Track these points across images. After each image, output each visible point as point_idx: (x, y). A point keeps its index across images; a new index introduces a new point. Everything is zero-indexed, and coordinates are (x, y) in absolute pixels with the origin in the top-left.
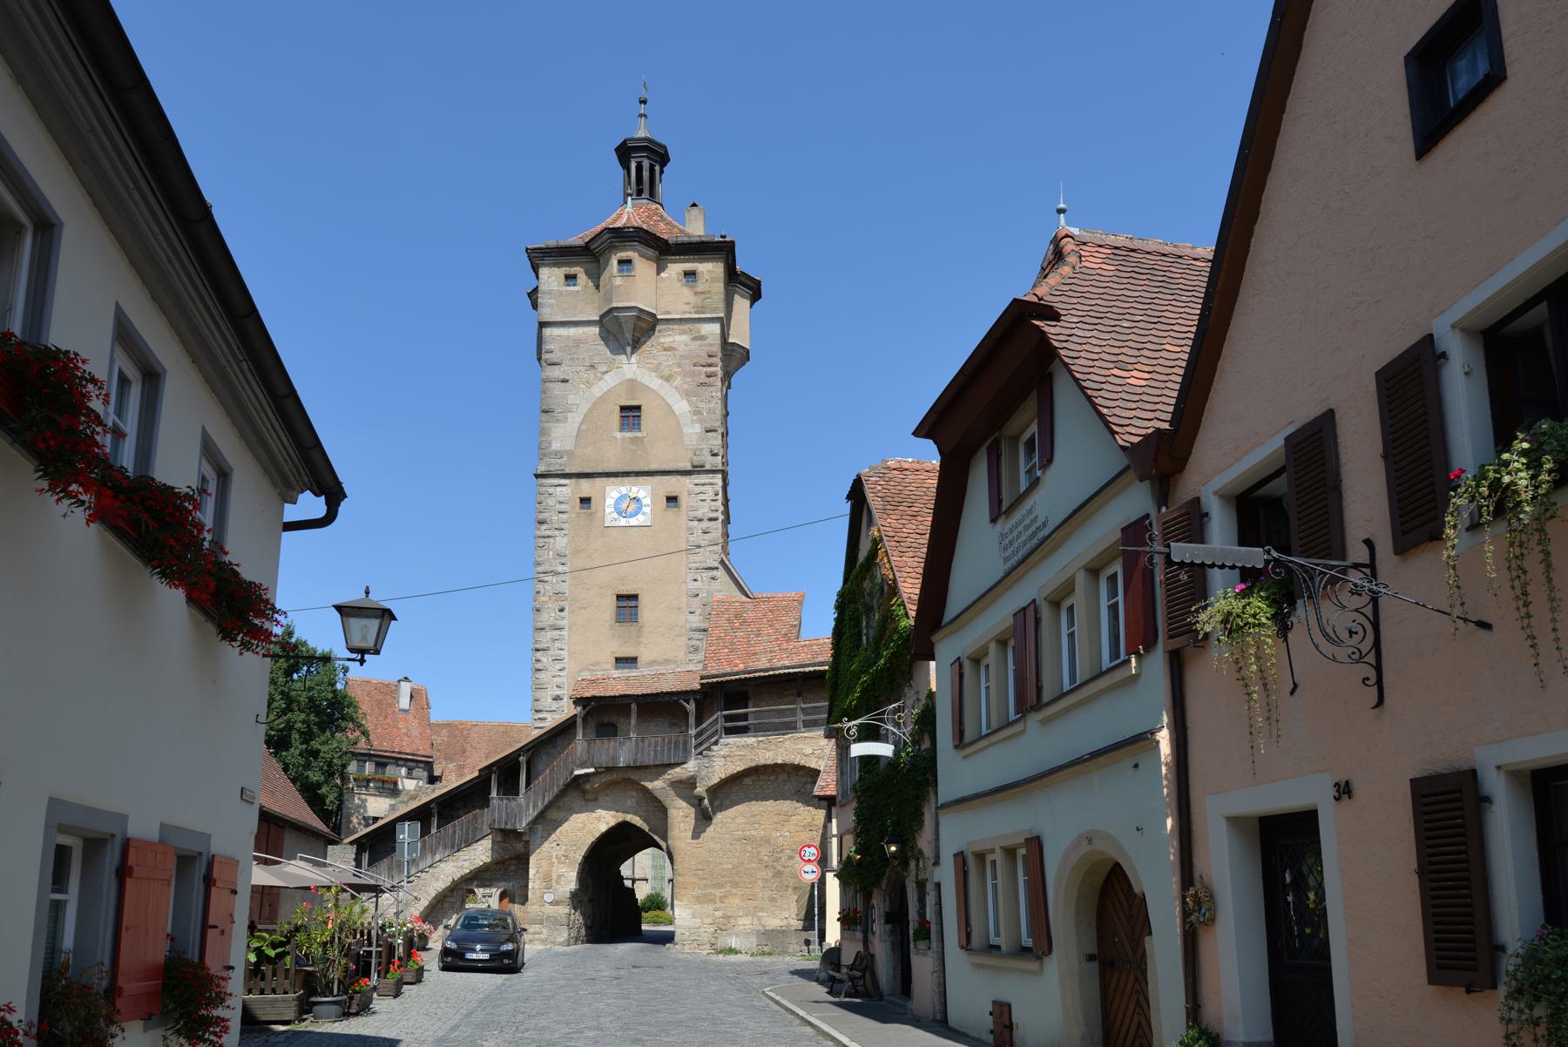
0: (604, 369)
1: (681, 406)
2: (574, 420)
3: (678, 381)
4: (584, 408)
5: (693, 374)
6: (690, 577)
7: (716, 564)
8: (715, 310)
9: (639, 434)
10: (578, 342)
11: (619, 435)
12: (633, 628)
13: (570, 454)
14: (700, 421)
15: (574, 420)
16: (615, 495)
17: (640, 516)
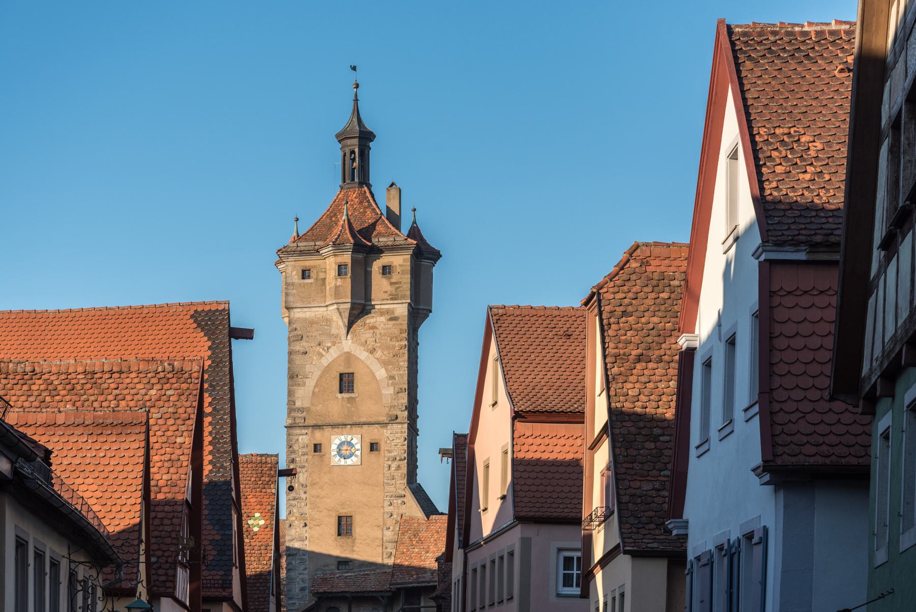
0: (329, 345)
1: (381, 373)
2: (311, 383)
3: (379, 353)
4: (317, 374)
5: (388, 348)
6: (387, 503)
7: (403, 493)
8: (403, 297)
9: (352, 395)
10: (311, 322)
11: (339, 396)
12: (349, 541)
13: (308, 410)
14: (393, 384)
15: (311, 383)
16: (337, 442)
17: (353, 458)
